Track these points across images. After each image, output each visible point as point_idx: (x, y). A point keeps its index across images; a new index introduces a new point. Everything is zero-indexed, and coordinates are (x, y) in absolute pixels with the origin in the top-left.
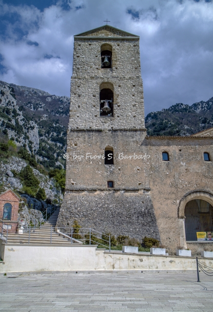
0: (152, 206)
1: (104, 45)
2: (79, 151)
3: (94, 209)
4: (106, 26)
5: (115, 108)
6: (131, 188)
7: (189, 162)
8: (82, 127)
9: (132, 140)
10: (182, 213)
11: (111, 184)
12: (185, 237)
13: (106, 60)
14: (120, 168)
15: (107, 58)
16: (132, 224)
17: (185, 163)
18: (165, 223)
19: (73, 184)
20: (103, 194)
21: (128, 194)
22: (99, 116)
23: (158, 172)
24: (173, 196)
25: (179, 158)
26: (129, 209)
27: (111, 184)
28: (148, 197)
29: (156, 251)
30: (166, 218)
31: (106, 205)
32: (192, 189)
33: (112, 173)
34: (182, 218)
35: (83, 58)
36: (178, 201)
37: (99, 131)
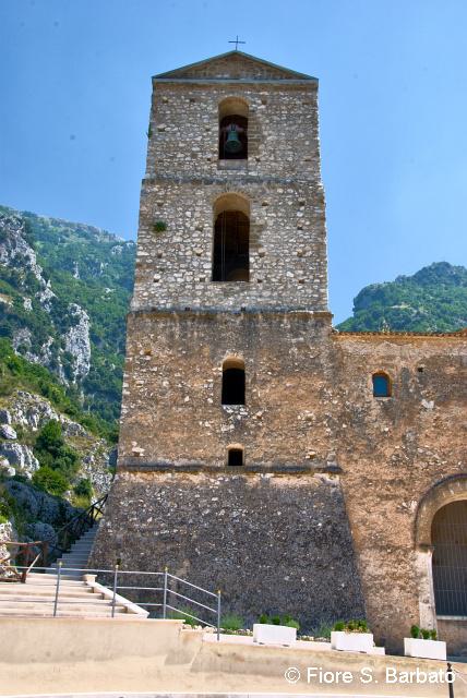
0: (345, 516)
1: (229, 101)
2: (155, 369)
3: (191, 521)
4: (234, 57)
5: (252, 260)
7: (443, 402)
9: (294, 341)
10: (425, 536)
11: (235, 458)
12: (432, 603)
13: (233, 137)
15: (235, 140)
16: (290, 563)
17: (432, 403)
18: (379, 563)
19: (137, 454)
20: (216, 482)
21: (282, 481)
23: (362, 424)
24: (401, 491)
25: (418, 390)
26: (280, 525)
27: (235, 458)
28: (333, 490)
29: (344, 640)
30: (382, 548)
31: (222, 512)
32: (452, 470)
33: (241, 426)
34: (424, 547)
35: (175, 133)
36: (414, 505)
37: (209, 317)
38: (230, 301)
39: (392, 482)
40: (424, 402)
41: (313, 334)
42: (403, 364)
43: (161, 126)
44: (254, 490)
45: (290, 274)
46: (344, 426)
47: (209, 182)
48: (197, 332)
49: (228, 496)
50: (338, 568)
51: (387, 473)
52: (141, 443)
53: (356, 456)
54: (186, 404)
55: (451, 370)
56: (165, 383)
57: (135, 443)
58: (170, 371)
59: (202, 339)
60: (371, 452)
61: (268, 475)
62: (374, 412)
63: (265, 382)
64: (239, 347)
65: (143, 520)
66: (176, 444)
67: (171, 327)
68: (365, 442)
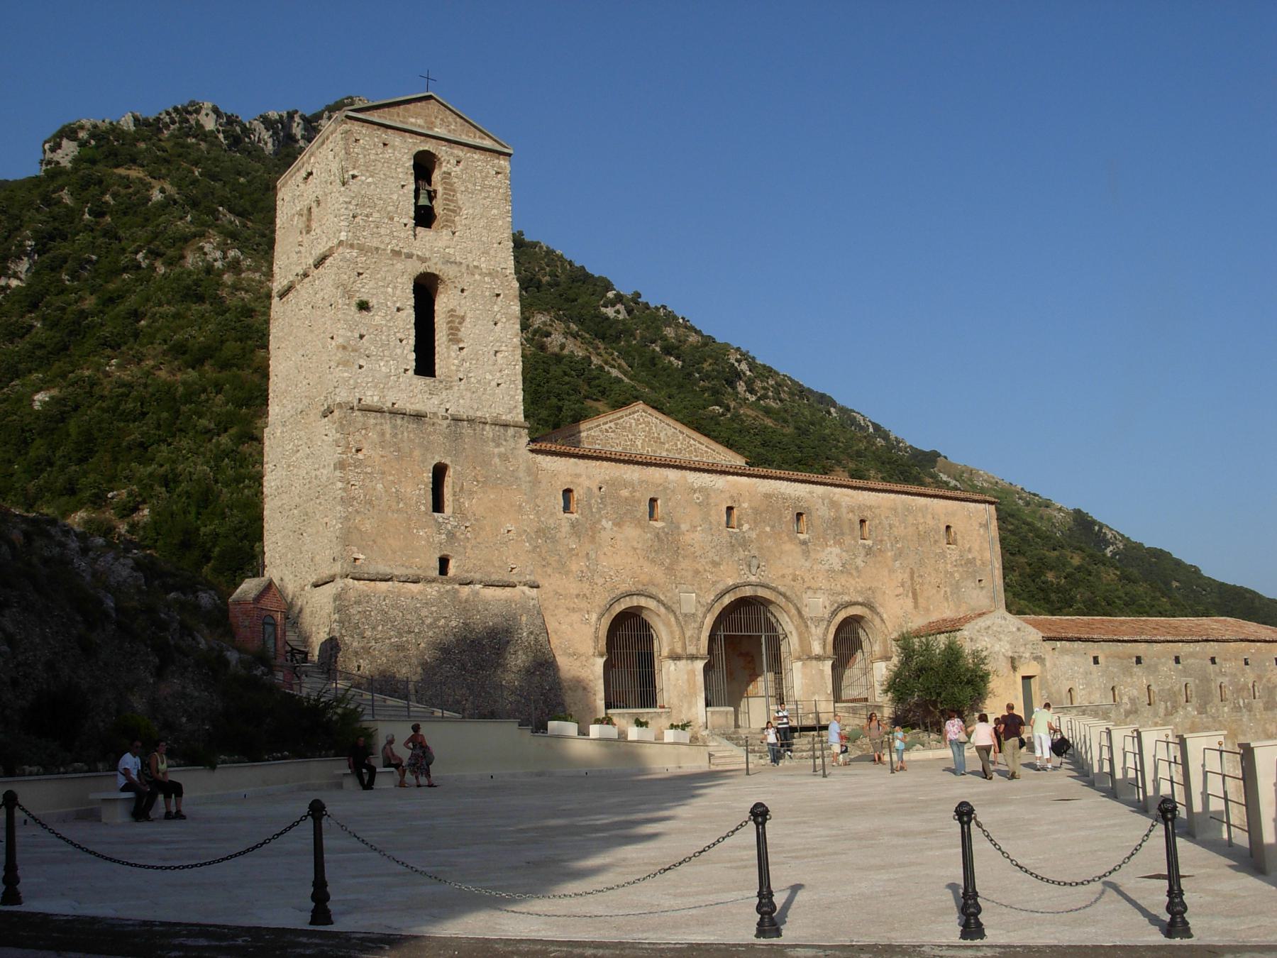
2: (369, 470)
3: (417, 630)
6: (495, 577)
7: (618, 524)
8: (371, 398)
9: (496, 450)
14: (467, 524)
20: (432, 591)
21: (490, 592)
22: (411, 372)
23: (554, 540)
24: (584, 604)
25: (599, 510)
28: (532, 602)
31: (442, 622)
32: (624, 588)
34: (601, 655)
35: (369, 184)
36: (594, 617)
37: (419, 417)
38: (436, 401)
39: (577, 596)
40: (604, 522)
41: (513, 445)
42: (587, 483)
43: (355, 172)
44: (466, 601)
45: (489, 377)
46: (540, 541)
47: (409, 256)
48: (408, 430)
49: (446, 606)
50: (543, 674)
51: (574, 587)
52: (362, 551)
53: (549, 571)
54: (399, 511)
55: (625, 493)
56: (380, 486)
57: (355, 549)
58: (383, 473)
59: (411, 441)
60: (563, 569)
61: (478, 587)
62: (564, 530)
63: (471, 493)
64: (448, 453)
65: (374, 628)
66: (394, 552)
67: (381, 424)
68: (557, 557)
